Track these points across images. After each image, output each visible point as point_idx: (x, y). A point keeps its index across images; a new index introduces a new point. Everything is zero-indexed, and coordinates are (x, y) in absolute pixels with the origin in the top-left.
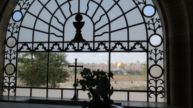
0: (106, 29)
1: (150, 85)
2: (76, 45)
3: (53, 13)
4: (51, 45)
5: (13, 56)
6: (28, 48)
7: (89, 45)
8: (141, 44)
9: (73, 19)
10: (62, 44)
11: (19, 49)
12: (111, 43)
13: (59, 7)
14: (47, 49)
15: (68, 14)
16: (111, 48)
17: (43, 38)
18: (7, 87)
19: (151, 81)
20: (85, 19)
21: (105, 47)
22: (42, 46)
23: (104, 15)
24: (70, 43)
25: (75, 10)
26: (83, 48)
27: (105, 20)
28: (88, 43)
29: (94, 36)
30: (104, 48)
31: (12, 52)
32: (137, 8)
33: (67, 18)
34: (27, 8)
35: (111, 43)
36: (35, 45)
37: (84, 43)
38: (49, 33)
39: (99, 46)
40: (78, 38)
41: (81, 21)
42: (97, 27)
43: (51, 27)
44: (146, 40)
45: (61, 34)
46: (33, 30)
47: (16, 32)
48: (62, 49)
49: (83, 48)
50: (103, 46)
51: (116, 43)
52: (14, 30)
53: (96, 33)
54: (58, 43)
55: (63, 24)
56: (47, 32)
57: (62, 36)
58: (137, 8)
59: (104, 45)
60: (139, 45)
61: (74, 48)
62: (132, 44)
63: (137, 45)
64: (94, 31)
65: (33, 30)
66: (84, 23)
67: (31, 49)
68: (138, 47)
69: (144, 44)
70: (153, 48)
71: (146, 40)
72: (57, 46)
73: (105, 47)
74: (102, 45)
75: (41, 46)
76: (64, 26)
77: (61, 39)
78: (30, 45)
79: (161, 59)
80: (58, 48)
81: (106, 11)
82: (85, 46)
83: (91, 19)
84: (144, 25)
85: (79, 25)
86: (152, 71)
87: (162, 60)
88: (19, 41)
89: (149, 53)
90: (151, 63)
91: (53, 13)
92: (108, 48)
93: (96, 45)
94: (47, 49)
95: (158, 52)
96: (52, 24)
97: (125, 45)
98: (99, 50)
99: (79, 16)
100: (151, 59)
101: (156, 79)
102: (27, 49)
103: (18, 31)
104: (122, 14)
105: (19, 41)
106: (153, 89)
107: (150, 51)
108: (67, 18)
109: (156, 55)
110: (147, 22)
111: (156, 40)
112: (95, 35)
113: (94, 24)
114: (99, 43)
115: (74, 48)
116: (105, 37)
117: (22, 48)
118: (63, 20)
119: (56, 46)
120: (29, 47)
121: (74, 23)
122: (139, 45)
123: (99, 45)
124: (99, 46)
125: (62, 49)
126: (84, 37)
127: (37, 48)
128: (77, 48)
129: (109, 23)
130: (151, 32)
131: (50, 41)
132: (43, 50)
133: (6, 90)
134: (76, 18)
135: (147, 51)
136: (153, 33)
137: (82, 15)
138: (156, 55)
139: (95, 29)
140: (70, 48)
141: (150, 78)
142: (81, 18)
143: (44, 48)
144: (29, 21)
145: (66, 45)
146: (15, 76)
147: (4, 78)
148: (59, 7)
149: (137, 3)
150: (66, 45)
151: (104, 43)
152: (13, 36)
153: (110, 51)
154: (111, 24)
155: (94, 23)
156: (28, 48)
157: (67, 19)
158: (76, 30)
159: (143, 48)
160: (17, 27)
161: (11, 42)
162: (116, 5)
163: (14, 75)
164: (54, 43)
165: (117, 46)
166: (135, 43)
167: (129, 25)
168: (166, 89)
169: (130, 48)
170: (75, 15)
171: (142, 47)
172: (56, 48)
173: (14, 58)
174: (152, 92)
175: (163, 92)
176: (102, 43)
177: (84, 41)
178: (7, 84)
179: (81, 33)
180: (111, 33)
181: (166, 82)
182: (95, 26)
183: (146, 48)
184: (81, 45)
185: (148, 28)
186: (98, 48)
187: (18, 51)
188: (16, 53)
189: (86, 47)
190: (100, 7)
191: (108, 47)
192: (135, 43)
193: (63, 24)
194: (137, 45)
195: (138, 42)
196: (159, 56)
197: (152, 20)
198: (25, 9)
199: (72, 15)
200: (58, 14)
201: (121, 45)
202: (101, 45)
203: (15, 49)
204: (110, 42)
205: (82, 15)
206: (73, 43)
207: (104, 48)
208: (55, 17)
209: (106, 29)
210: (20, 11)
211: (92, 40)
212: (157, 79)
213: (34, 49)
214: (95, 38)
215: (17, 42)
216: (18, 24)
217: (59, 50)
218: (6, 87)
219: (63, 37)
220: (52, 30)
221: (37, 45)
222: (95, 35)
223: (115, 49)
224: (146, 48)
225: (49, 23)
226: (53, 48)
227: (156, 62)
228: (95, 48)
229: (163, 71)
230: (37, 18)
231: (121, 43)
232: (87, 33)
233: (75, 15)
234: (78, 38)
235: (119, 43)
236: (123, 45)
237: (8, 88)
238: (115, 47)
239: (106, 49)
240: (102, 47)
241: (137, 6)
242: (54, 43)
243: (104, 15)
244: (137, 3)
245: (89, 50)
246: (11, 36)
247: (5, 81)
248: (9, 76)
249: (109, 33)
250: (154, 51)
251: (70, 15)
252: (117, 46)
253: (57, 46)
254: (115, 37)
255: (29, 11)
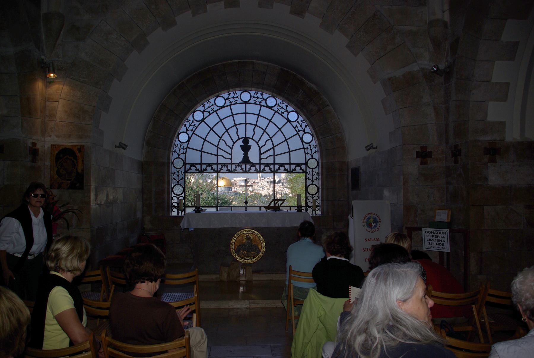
0: (271, 153)
1: (308, 201)
2: (243, 166)
3: (220, 136)
4: (220, 166)
5: (181, 176)
6: (197, 169)
7: (255, 167)
8: (300, 166)
9: (240, 143)
10: (230, 165)
11: (186, 170)
12: (276, 165)
13: (227, 130)
14: (216, 170)
15: (235, 138)
16: (275, 170)
17: (212, 159)
18: (176, 207)
19: (309, 198)
20: (251, 143)
21: (270, 169)
22: (210, 168)
23: (269, 140)
24: (239, 165)
25: (242, 135)
26: (250, 169)
27: (269, 145)
28: (255, 165)
29: (260, 159)
30: (269, 170)
31: (180, 173)
32: (297, 135)
33: (234, 141)
34: (194, 130)
35: (276, 165)
36: (204, 167)
37: (251, 165)
38: (217, 155)
39: (264, 168)
40: (246, 160)
41: (248, 145)
42: (263, 150)
43: (218, 149)
44: (304, 162)
45: (230, 156)
46: (200, 152)
47: (183, 153)
48: (230, 170)
49: (250, 169)
50: (268, 168)
51: (280, 165)
52: (181, 151)
53: (262, 156)
54: (227, 165)
55: (231, 147)
56: (216, 154)
57: (230, 158)
58: (297, 135)
59: (269, 167)
60: (299, 167)
61: (242, 169)
62: (293, 167)
63: (297, 167)
64: (261, 154)
65: (200, 152)
66: (250, 147)
67: (200, 170)
68: (298, 169)
69: (303, 167)
70: (310, 170)
71: (304, 162)
72: (226, 167)
73: (270, 169)
74: (267, 167)
75: (209, 167)
76: (232, 148)
77: (229, 161)
78: (198, 167)
79: (316, 179)
80: (226, 169)
81: (271, 137)
82: (252, 168)
83: (257, 143)
84: (303, 149)
85: (246, 148)
86: (309, 189)
87: (317, 180)
88: (187, 162)
89: (307, 174)
90: (309, 182)
91: (220, 136)
92: (273, 170)
93: (262, 167)
94: (216, 170)
95: (314, 173)
96: (219, 146)
97: (287, 167)
98: (264, 171)
99: (246, 140)
100: (309, 179)
101: (312, 196)
102: (195, 170)
103: (185, 152)
104: (285, 139)
105: (187, 162)
106: (310, 204)
107: (308, 173)
108: (234, 141)
109: (313, 176)
110: (305, 147)
111: (312, 163)
112: (261, 158)
113: (260, 148)
114: (265, 165)
115: (242, 169)
116: (270, 160)
117: (190, 169)
118: (230, 143)
119: (224, 167)
120: (198, 168)
121: (241, 146)
122: (299, 167)
123: (265, 167)
124: (264, 168)
125: (230, 170)
126: (251, 160)
127: (206, 169)
128: (244, 170)
129: (274, 147)
130: (308, 157)
131: (219, 162)
132: (212, 171)
133: (175, 210)
134: (243, 142)
135: (305, 172)
136: (311, 157)
137: (249, 139)
138: (313, 176)
139: (262, 152)
140: (239, 169)
141: (308, 195)
142: (248, 142)
143: (212, 169)
144: (196, 143)
145: (234, 167)
146: (184, 197)
147: (172, 198)
148: (227, 130)
149: (298, 131)
150: (234, 167)
151: (269, 165)
152: (180, 157)
153: (274, 172)
154: (275, 148)
155: (260, 147)
156: (197, 169)
157: (234, 143)
158: (244, 153)
159: (302, 170)
160: (184, 148)
161: (178, 163)
162: (280, 131)
163: (183, 195)
164: (222, 165)
165: (281, 168)
166: (296, 165)
167: (291, 150)
168: (320, 204)
169: (291, 170)
170: (242, 139)
171: (301, 169)
172: (225, 169)
173: (182, 179)
174: (310, 207)
175: (318, 206)
176: (267, 165)
177: (251, 163)
178: (175, 204)
179: (248, 155)
180: (275, 157)
181: (320, 198)
182: (261, 150)
183: (305, 170)
184: (248, 166)
185: (306, 152)
186: (264, 170)
187: (186, 172)
188: (184, 174)
189: (253, 169)
190: (265, 133)
191: (272, 169)
192: (296, 165)
193: (231, 147)
194: (297, 167)
195: (298, 165)
196: (315, 177)
197: (310, 146)
198: (192, 130)
199: (239, 139)
200: (226, 137)
201: (284, 167)
202: (266, 167)
203: (183, 170)
204: (274, 164)
205: (249, 139)
206: (241, 165)
207: (269, 170)
208: (223, 140)
209: (271, 153)
210: (186, 132)
211: (258, 162)
212: (313, 196)
213: (202, 170)
214: (261, 160)
215: (185, 163)
216: (185, 145)
217: (227, 171)
218: (175, 207)
219: (231, 159)
220: (220, 152)
221: (206, 167)
222: (261, 158)
223: (279, 171)
224: (305, 170)
225: (217, 145)
226: (221, 169)
227: (313, 182)
228: (261, 170)
229: (318, 188)
230: (205, 140)
231: (284, 165)
232: (254, 156)
233: (242, 139)
234: (246, 160)
235: (282, 165)
236: (285, 167)
237: (177, 208)
238: (279, 169)
239: (271, 171)
240: (267, 169)
241: (298, 134)
242: (222, 165)
243: (269, 140)
244: (298, 131)
245: (256, 171)
246: (177, 157)
247: (173, 201)
248: (177, 196)
249: (273, 157)
250: (311, 173)
251: (238, 138)
252: (281, 168)
253: (226, 167)
254: (278, 160)
255: (195, 132)
